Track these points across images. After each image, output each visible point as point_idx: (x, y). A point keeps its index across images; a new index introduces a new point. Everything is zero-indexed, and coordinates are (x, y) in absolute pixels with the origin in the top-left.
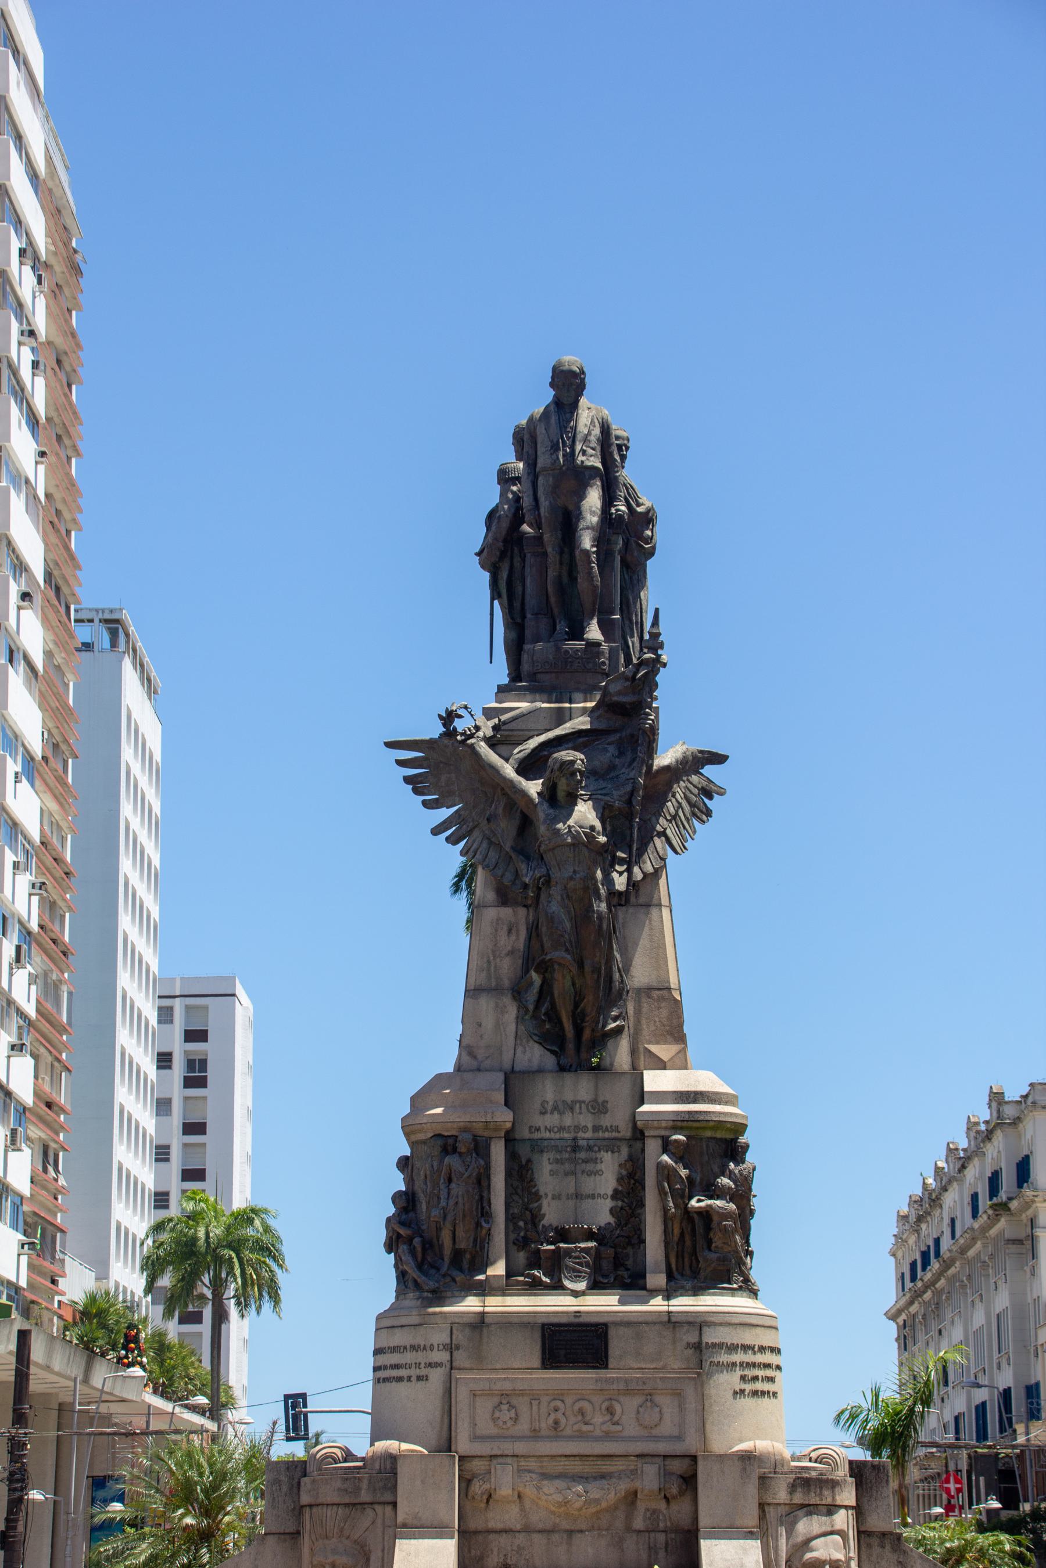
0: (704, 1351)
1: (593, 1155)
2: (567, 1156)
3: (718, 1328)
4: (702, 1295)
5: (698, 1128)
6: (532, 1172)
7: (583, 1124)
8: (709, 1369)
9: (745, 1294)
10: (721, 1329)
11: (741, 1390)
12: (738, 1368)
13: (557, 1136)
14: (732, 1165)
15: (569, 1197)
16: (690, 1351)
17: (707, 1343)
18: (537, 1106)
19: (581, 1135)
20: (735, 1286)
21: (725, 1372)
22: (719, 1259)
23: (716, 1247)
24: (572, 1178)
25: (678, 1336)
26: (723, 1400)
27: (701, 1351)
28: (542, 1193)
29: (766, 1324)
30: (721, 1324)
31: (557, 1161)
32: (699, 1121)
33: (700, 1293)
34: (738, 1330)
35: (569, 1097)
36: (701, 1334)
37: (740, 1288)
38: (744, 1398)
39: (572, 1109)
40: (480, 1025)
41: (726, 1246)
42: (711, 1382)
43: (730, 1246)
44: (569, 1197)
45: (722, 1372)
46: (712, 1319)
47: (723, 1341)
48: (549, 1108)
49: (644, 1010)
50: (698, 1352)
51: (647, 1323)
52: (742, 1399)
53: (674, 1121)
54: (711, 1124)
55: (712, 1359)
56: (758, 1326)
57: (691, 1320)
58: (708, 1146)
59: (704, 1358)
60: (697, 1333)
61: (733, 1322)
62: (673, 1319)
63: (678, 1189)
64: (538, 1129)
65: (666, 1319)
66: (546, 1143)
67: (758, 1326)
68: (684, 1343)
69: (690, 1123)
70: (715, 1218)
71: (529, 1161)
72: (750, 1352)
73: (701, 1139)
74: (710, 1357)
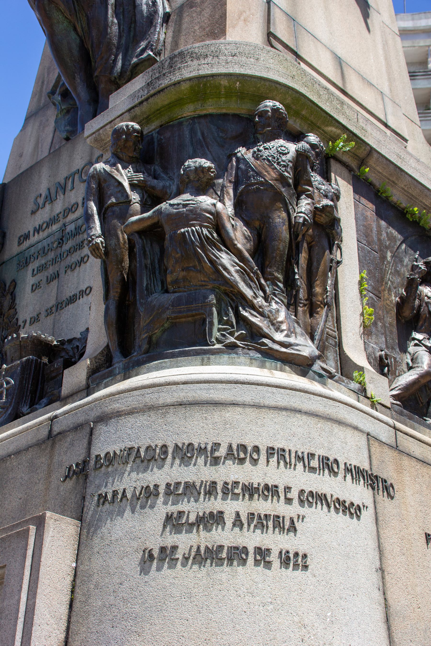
0: (92, 474)
1: (79, 239)
2: (51, 255)
3: (123, 420)
4: (136, 375)
5: (171, 106)
6: (13, 298)
7: (73, 201)
8: (95, 511)
9: (242, 359)
10: (131, 420)
11: (163, 549)
12: (161, 499)
13: (46, 233)
14: (242, 151)
15: (49, 312)
16: (70, 484)
17: (98, 457)
18: (31, 206)
19: (72, 217)
20: (217, 346)
21: (128, 513)
22: (177, 303)
23: (176, 282)
24: (54, 283)
25: (56, 459)
26: (116, 580)
27: (86, 477)
28: (20, 323)
29: (267, 402)
30: (131, 412)
31: (42, 268)
32: (162, 90)
33: (134, 372)
34: (171, 417)
35: (63, 173)
36: (90, 443)
37: (232, 347)
38: (172, 566)
39: (64, 189)
40: (21, 156)
41: (192, 274)
42: (96, 540)
43: (201, 271)
44: (49, 312)
45: (121, 513)
46: (116, 406)
47: (129, 444)
48: (41, 201)
49: (184, 26)
50: (81, 481)
51: (18, 453)
52: (166, 570)
53: (129, 110)
54: (185, 86)
55: (103, 491)
56: (234, 404)
57: (81, 419)
58: (193, 131)
59: (89, 491)
60: (85, 441)
61: (161, 401)
62: (56, 429)
63: (113, 205)
64: (27, 237)
65: (44, 433)
66: (33, 250)
67: (234, 404)
68: (64, 471)
69: (150, 100)
70: (167, 228)
71: (14, 283)
72: (201, 461)
73: (181, 124)
74: (99, 487)
